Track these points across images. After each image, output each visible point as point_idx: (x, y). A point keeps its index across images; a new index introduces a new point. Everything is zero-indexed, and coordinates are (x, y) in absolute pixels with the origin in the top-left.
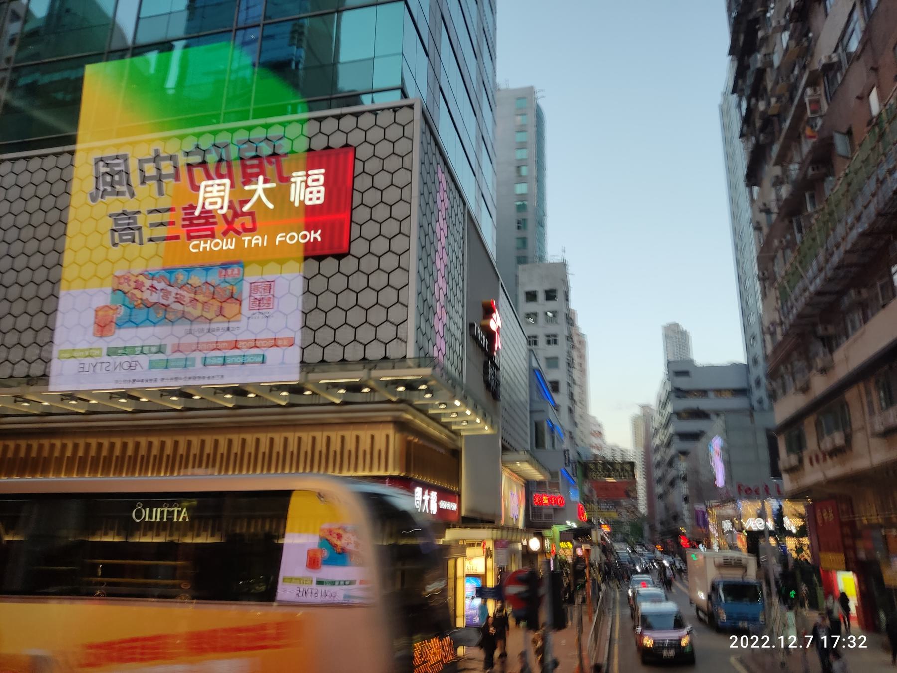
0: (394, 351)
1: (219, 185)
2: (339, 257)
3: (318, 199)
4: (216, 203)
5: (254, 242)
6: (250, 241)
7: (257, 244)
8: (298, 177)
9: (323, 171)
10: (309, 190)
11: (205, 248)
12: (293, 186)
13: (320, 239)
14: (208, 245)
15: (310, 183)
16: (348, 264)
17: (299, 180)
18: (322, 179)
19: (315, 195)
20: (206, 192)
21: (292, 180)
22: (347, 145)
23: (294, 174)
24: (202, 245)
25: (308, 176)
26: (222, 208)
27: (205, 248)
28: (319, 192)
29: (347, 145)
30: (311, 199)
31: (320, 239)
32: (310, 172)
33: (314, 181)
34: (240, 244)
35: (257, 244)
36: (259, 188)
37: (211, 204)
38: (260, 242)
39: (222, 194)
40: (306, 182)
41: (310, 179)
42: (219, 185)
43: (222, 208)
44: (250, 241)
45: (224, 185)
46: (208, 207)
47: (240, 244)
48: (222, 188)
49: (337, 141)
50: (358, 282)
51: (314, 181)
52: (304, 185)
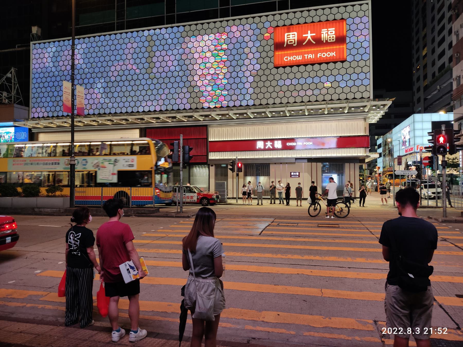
0: (366, 95)
1: (293, 35)
2: (342, 62)
3: (333, 40)
4: (292, 42)
5: (309, 57)
6: (307, 56)
7: (310, 57)
8: (324, 31)
9: (334, 29)
10: (329, 36)
11: (290, 59)
12: (322, 35)
13: (335, 55)
14: (291, 58)
15: (329, 34)
16: (346, 65)
17: (324, 32)
18: (334, 32)
19: (331, 39)
20: (287, 38)
21: (322, 32)
22: (342, 19)
23: (323, 30)
24: (289, 58)
25: (328, 31)
26: (295, 43)
27: (290, 59)
28: (333, 37)
29: (342, 19)
30: (330, 40)
31: (335, 55)
32: (329, 29)
33: (331, 33)
34: (304, 57)
35: (310, 57)
36: (309, 36)
37: (290, 42)
38: (311, 56)
39: (294, 38)
40: (327, 33)
41: (329, 32)
42: (293, 35)
43: (295, 43)
44: (307, 56)
45: (294, 34)
46: (289, 43)
47: (304, 57)
48: (294, 36)
49: (338, 17)
50: (350, 71)
51: (331, 33)
52: (327, 34)
